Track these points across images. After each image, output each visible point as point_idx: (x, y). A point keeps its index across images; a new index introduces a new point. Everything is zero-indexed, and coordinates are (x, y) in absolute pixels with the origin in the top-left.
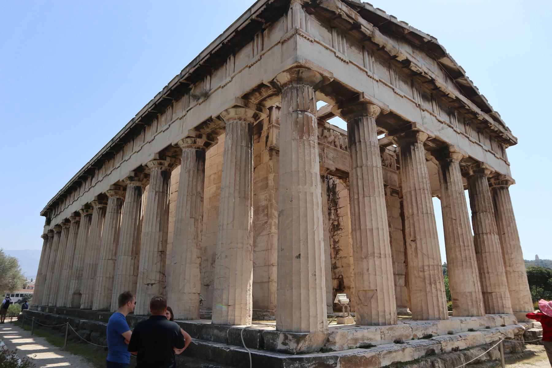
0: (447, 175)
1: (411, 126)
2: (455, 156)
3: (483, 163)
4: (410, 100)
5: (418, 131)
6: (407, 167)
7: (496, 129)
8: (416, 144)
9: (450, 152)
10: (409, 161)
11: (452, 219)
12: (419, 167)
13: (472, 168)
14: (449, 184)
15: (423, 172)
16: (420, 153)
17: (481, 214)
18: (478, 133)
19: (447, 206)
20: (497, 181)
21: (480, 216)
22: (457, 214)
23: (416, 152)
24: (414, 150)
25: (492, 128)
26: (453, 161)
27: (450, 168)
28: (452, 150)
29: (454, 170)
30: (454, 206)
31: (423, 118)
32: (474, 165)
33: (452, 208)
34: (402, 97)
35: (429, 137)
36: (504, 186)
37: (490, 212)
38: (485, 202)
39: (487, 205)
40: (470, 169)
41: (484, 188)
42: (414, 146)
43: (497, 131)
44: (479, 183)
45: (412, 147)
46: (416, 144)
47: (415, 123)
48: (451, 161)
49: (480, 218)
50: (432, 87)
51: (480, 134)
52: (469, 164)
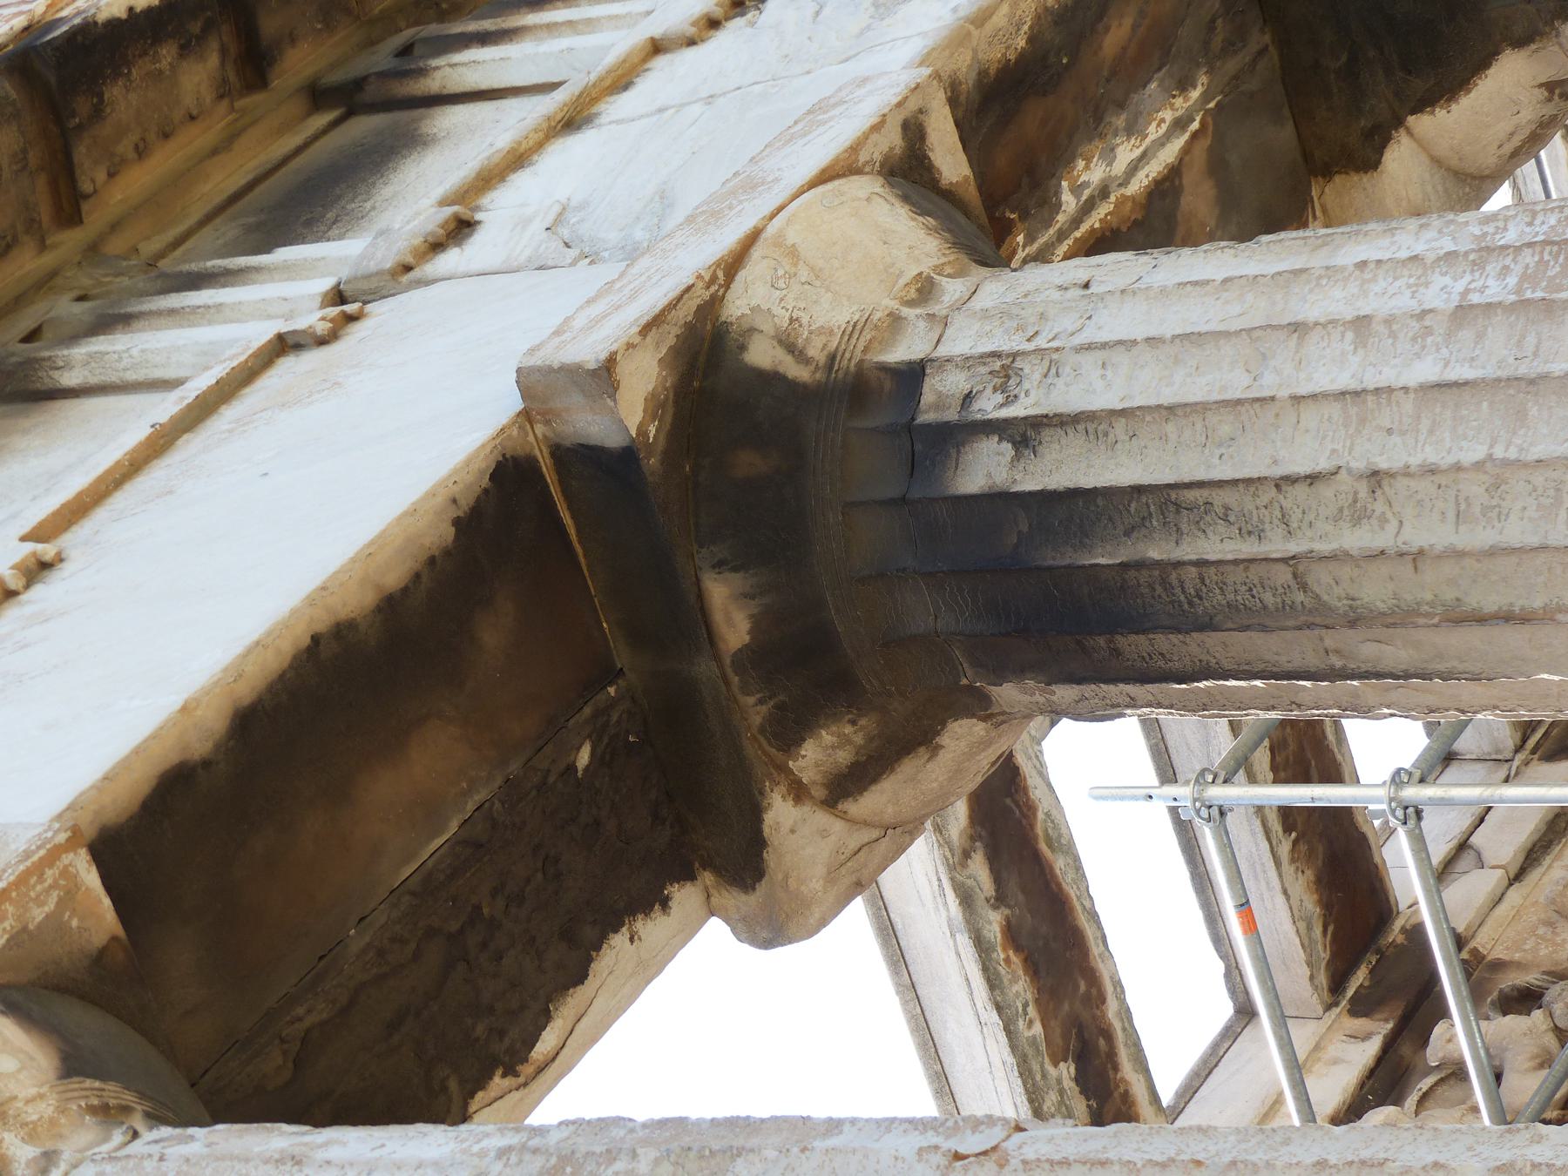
1: (580, 460)
4: (160, 443)
5: (703, 349)
6: (1329, 586)
8: (941, 393)
10: (1215, 546)
12: (1332, 367)
15: (1442, 291)
16: (1114, 323)
23: (1067, 397)
24: (1024, 435)
31: (565, 239)
34: (38, 569)
35: (908, 171)
42: (962, 432)
45: (985, 469)
46: (941, 393)
47: (539, 387)
50: (197, 76)
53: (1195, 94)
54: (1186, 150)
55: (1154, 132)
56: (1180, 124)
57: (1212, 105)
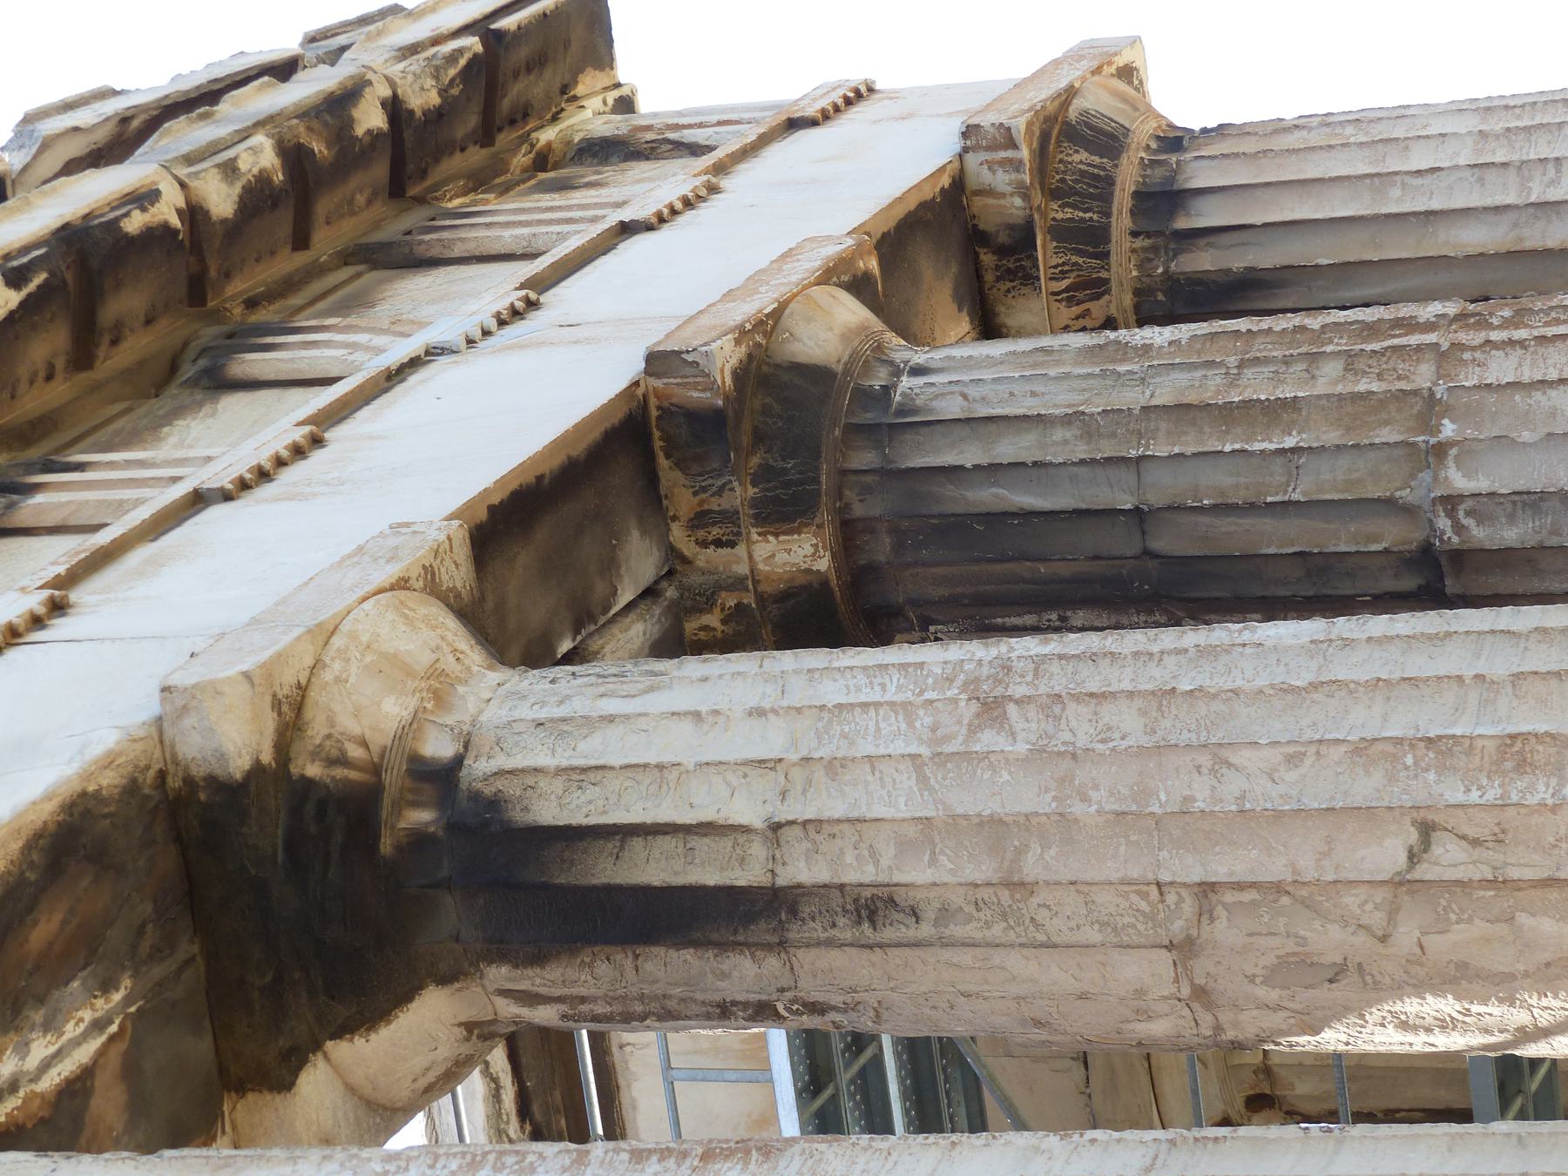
0: (654, 868)
2: (366, 712)
3: (657, 361)
7: (260, 156)
9: (273, 780)
11: (1399, 883)
13: (718, 527)
14: (800, 870)
17: (1458, 480)
18: (219, 383)
19: (1184, 949)
20: (1046, 253)
21: (1486, 504)
22: (1318, 786)
25: (221, 200)
26: (438, 747)
27: (548, 811)
28: (234, 740)
29: (589, 750)
30: (1186, 824)
32: (681, 496)
33: (1221, 867)
36: (1128, 176)
37: (1445, 357)
38: (1277, 411)
39: (1329, 379)
40: (735, 561)
41: (1057, 400)
43: (293, 155)
44: (970, 455)
48: (440, 778)
49: (1529, 501)
51: (253, 363)
52: (640, 563)
53: (117, 997)
54: (102, 1052)
55: (71, 1030)
56: (98, 1025)
57: (133, 1009)
